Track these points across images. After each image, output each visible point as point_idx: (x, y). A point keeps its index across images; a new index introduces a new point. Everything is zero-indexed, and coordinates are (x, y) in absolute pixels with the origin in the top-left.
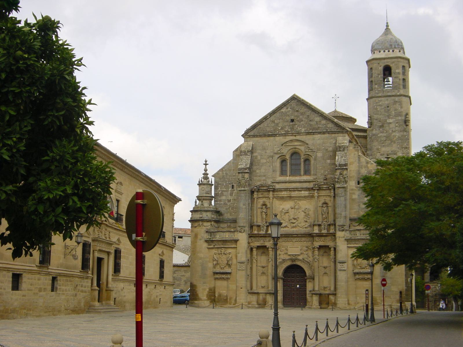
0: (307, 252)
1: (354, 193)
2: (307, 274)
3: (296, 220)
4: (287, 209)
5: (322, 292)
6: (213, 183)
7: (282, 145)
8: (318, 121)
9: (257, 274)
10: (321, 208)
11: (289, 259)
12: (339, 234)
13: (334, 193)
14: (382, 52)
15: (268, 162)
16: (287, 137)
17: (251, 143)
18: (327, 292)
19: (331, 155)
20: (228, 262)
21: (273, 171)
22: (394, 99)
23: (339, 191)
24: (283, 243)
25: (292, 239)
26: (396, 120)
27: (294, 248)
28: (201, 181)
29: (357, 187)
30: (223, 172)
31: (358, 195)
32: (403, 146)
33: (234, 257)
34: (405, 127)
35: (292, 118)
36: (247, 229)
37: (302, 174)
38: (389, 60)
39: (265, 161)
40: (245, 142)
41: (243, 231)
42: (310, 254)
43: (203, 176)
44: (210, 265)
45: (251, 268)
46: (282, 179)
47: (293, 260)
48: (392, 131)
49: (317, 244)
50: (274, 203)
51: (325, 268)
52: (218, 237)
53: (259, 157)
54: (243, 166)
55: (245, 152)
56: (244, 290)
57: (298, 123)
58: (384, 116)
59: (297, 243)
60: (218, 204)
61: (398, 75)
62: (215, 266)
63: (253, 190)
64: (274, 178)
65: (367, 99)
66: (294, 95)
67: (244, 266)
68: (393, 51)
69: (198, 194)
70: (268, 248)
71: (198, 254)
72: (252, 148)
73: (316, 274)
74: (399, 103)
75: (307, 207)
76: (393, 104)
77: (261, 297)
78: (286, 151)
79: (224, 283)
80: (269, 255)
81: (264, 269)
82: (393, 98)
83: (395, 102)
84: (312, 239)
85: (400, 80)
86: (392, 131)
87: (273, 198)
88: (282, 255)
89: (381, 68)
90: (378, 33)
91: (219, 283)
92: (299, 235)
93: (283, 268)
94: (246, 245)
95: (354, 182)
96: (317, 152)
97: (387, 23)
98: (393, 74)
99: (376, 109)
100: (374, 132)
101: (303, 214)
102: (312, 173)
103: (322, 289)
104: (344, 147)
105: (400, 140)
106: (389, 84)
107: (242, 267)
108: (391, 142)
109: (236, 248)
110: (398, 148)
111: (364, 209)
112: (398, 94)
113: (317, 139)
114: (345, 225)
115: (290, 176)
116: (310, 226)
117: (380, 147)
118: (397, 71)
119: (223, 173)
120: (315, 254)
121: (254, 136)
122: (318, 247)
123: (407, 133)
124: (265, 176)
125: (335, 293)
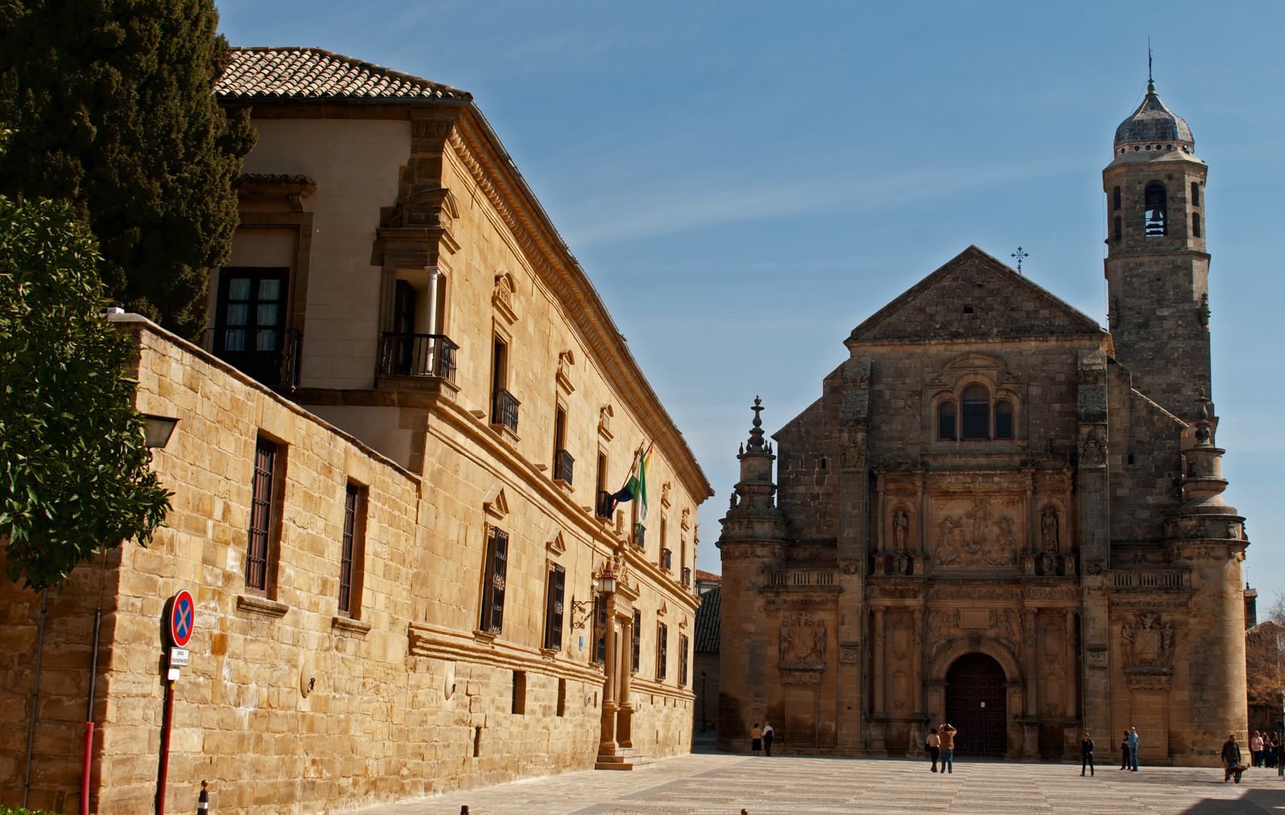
1: (1120, 485)
2: (1008, 676)
3: (979, 546)
4: (955, 518)
6: (775, 453)
7: (943, 366)
8: (1031, 309)
10: (1040, 518)
11: (962, 639)
12: (1091, 581)
13: (1074, 484)
14: (1143, 149)
15: (910, 406)
16: (956, 348)
17: (868, 361)
19: (1063, 391)
20: (815, 645)
21: (922, 428)
22: (1173, 262)
23: (1088, 480)
26: (1178, 312)
28: (748, 448)
29: (1127, 470)
30: (799, 427)
31: (1131, 489)
32: (1196, 374)
33: (830, 633)
34: (1199, 327)
35: (967, 303)
36: (863, 565)
37: (992, 436)
38: (1158, 168)
39: (901, 403)
40: (852, 356)
41: (853, 570)
42: (1015, 628)
43: (751, 436)
44: (772, 651)
46: (944, 445)
48: (1170, 336)
49: (1032, 604)
50: (925, 504)
52: (790, 582)
53: (887, 394)
54: (850, 415)
55: (855, 381)
56: (855, 711)
57: (982, 314)
58: (1148, 301)
60: (786, 503)
61: (1183, 204)
62: (782, 652)
63: (875, 472)
64: (925, 443)
65: (1106, 261)
66: (972, 248)
67: (854, 656)
68: (1169, 147)
69: (738, 481)
70: (912, 613)
71: (743, 625)
72: (872, 371)
73: (1029, 677)
74: (1185, 271)
75: (1005, 513)
76: (1172, 275)
77: (894, 732)
78: (954, 380)
79: (807, 695)
82: (1171, 258)
83: (1176, 269)
84: (1019, 591)
85: (1186, 215)
86: (1170, 336)
87: (923, 493)
89: (1141, 188)
90: (1129, 105)
91: (795, 695)
93: (950, 661)
94: (860, 605)
95: (1120, 457)
96: (1028, 385)
97: (1151, 81)
98: (1170, 204)
99: (1131, 283)
100: (1126, 338)
101: (996, 529)
102: (1017, 432)
104: (1095, 372)
105: (1189, 358)
106: (1158, 226)
108: (1167, 364)
109: (837, 610)
110: (1184, 377)
111: (1144, 520)
112: (1183, 250)
113: (1030, 353)
114: (1102, 561)
115: (962, 440)
116: (1014, 560)
117: (1139, 375)
118: (1179, 195)
119: (800, 431)
120: (1028, 627)
121: (875, 340)
122: (1036, 611)
123: (1206, 343)
124: (901, 440)
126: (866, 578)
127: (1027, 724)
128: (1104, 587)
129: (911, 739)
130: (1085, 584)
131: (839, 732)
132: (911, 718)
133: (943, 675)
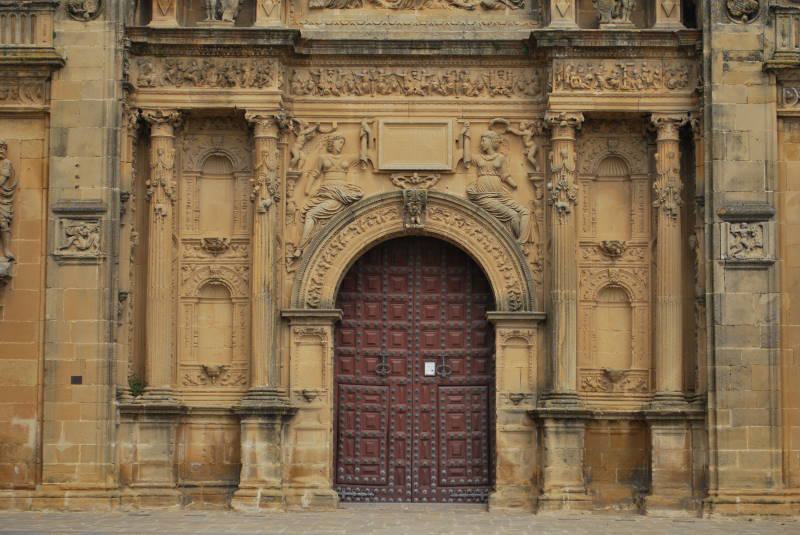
0: (497, 158)
2: (500, 292)
5: (597, 404)
9: (174, 288)
18: (630, 405)
24: (344, 97)
25: (399, 71)
33: (28, 178)
42: (517, 167)
45: (142, 256)
47: (406, 204)
49: (567, 104)
51: (610, 252)
56: (93, 390)
77: (200, 440)
80: (251, 170)
81: (223, 258)
84: (529, 74)
88: (341, 175)
92: (460, 51)
103: (595, 384)
107: (84, 243)
109: (45, 115)
120: (557, 163)
122: (580, 118)
126: (128, 31)
127: (557, 417)
128: (767, 55)
129: (246, 461)
130: (716, 44)
131: (47, 446)
132: (247, 403)
133: (329, 292)
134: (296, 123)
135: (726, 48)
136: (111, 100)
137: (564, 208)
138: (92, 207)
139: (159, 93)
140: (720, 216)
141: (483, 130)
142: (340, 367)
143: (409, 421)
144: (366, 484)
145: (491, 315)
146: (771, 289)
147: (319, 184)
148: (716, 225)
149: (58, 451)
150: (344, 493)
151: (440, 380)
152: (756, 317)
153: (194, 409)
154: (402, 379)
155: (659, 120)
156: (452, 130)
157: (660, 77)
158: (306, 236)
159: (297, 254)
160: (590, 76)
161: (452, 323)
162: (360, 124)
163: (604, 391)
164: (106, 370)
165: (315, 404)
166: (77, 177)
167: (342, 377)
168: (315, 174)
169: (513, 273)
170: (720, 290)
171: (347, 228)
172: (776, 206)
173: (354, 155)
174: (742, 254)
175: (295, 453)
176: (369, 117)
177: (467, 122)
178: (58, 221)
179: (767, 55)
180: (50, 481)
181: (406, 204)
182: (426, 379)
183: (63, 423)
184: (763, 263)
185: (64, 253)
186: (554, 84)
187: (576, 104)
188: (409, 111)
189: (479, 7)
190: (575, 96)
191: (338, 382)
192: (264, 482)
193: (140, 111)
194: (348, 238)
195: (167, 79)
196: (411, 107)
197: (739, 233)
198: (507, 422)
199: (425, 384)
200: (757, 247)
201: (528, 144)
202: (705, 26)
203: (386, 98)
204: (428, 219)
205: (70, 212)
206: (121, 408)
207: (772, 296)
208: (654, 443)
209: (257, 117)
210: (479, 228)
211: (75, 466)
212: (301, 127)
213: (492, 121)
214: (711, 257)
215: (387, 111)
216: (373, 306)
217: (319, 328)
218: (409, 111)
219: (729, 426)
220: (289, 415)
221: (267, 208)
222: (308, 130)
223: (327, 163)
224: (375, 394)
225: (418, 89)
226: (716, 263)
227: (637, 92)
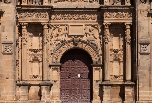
2: (94, 60)
5: (113, 82)
18: (121, 82)
27: (76, 27)
47: (75, 43)
51: (116, 52)
56: (11, 81)
59: (80, 20)
70: (43, 26)
103: (113, 78)
107: (8, 50)
120: (105, 33)
125: (132, 83)
126: (17, 6)
128: (149, 10)
129: (42, 94)
130: (138, 8)
133: (59, 60)
134: (52, 26)
135: (141, 9)
136: (14, 20)
137: (107, 42)
138: (10, 42)
139: (23, 19)
140: (139, 43)
141: (90, 27)
142: (61, 76)
143: (75, 86)
144: (66, 99)
145: (92, 65)
146: (150, 58)
147: (57, 38)
148: (138, 45)
149: (4, 93)
150: (62, 101)
151: (81, 78)
152: (146, 64)
153: (32, 84)
154: (74, 78)
155: (126, 24)
156: (84, 27)
157: (126, 15)
158: (54, 49)
159: (52, 52)
160: (112, 15)
161: (84, 66)
162: (65, 26)
163: (115, 80)
164: (13, 76)
165: (56, 83)
166: (7, 36)
167: (62, 77)
168: (56, 36)
169: (96, 56)
170: (139, 59)
171: (62, 47)
172: (151, 41)
173: (64, 32)
174: (144, 51)
175: (53, 93)
176: (67, 24)
177: (87, 25)
178: (3, 45)
179: (149, 10)
180: (2, 99)
181: (75, 43)
182: (78, 78)
183: (5, 87)
184: (148, 53)
185: (4, 52)
186: (105, 17)
187: (109, 21)
188: (75, 23)
189: (89, 2)
190: (109, 19)
191: (61, 78)
192: (46, 99)
193: (20, 23)
194: (63, 49)
195: (25, 16)
196: (75, 22)
197: (143, 47)
198: (95, 86)
199: (78, 79)
200: (147, 50)
201: (99, 29)
202: (136, 4)
203: (70, 20)
204: (79, 45)
205: (5, 44)
206: (16, 84)
207: (150, 60)
208: (125, 90)
209: (44, 24)
210: (89, 47)
211: (7, 97)
212: (53, 26)
213: (92, 25)
214: (137, 52)
215: (70, 23)
216: (68, 63)
217: (57, 67)
218: (75, 23)
219: (141, 87)
220: (51, 85)
221: (46, 43)
222: (54, 27)
223: (58, 34)
224: (68, 81)
225: (77, 18)
226: (138, 53)
227: (121, 18)
